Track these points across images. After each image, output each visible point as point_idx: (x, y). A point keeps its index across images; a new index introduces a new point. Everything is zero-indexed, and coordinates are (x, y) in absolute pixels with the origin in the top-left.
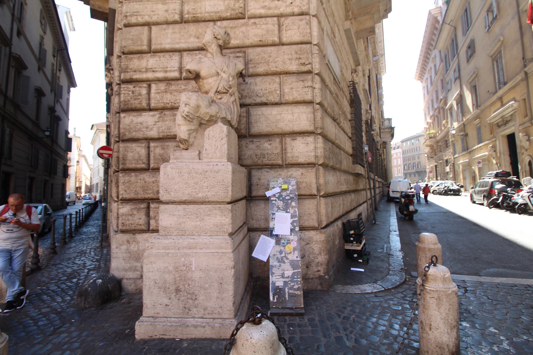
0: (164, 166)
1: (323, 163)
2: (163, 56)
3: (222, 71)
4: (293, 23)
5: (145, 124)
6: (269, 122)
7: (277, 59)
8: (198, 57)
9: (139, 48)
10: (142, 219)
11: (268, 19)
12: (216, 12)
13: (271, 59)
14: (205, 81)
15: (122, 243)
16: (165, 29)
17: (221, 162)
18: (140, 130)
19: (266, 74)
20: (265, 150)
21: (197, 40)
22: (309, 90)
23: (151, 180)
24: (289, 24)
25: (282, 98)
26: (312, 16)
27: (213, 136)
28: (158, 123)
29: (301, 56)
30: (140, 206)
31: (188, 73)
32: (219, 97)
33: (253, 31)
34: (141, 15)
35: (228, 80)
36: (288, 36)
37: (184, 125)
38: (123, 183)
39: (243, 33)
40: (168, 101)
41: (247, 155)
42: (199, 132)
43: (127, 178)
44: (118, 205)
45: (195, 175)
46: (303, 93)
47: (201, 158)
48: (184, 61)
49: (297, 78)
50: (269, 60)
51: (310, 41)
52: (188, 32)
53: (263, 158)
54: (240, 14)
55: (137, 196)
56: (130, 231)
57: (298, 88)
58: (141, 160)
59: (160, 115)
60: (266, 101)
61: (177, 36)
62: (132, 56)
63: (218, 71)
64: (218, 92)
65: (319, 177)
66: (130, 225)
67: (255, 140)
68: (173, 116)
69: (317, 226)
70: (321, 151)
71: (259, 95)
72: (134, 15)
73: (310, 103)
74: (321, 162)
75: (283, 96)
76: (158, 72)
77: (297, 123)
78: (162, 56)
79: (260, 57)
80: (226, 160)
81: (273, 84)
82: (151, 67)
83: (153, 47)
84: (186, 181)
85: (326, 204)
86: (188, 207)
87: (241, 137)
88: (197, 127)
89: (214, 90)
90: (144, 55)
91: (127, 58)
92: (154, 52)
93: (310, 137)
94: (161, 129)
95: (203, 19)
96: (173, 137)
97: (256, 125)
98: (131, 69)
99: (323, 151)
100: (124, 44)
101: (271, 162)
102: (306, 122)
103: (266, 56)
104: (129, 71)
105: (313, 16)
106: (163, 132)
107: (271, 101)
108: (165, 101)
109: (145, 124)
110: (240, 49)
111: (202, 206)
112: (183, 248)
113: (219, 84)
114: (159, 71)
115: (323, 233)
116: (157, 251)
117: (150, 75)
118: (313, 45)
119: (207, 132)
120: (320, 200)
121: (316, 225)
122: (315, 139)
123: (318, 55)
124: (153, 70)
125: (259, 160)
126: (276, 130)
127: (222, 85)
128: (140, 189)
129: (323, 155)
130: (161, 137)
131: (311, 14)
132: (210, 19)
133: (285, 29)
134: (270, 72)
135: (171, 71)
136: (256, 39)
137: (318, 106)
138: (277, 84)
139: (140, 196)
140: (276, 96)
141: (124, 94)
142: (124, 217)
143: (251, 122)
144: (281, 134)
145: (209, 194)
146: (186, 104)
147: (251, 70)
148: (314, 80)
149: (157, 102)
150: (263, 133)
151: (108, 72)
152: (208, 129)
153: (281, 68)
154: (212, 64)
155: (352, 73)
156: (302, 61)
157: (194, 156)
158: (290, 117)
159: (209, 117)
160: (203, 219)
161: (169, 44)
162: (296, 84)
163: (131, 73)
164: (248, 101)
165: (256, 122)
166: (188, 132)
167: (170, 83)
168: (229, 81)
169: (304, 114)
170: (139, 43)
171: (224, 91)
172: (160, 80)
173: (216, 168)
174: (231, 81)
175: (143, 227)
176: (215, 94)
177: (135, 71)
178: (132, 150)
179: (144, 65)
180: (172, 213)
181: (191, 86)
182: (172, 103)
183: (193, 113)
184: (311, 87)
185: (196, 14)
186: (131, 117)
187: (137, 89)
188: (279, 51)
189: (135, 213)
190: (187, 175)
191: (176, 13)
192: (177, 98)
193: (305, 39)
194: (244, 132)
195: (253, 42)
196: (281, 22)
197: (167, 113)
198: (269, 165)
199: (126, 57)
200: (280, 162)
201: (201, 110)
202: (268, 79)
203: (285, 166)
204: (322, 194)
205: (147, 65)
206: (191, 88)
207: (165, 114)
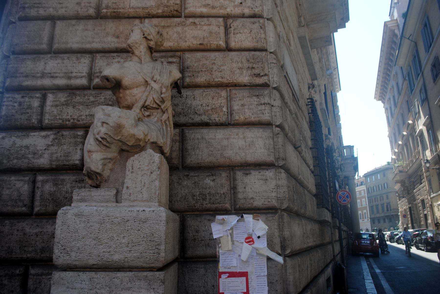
0: (63, 212)
1: (288, 207)
2: (68, 58)
4: (243, 25)
5: (31, 149)
6: (212, 149)
7: (222, 68)
8: (116, 60)
9: (36, 47)
11: (211, 19)
12: (143, 8)
13: (215, 67)
14: (128, 92)
16: (74, 25)
18: (24, 156)
19: (208, 86)
20: (206, 188)
21: (116, 40)
22: (266, 108)
23: (35, 231)
24: (238, 26)
26: (266, 19)
27: (140, 168)
28: (52, 148)
29: (254, 66)
31: (105, 80)
32: (147, 113)
33: (191, 32)
34: (44, 7)
35: (159, 92)
36: (237, 40)
37: (97, 151)
39: (178, 33)
40: (69, 117)
41: (180, 196)
48: (96, 65)
49: (250, 93)
50: (212, 68)
51: (265, 48)
53: (203, 199)
54: (175, 12)
58: (20, 200)
59: (55, 136)
60: (208, 121)
62: (25, 57)
63: (147, 80)
64: (146, 107)
65: (282, 228)
67: (192, 174)
68: (75, 137)
72: (34, 7)
73: (267, 125)
74: (285, 206)
75: (231, 115)
76: (58, 78)
78: (66, 58)
79: (201, 64)
80: (157, 204)
81: (218, 99)
82: (49, 72)
83: (55, 46)
86: (95, 276)
87: (173, 169)
89: (140, 104)
92: (55, 53)
93: (270, 171)
94: (55, 156)
95: (126, 15)
97: (193, 153)
98: (22, 73)
99: (286, 190)
101: (214, 206)
102: (263, 150)
103: (207, 63)
104: (18, 75)
106: (58, 160)
107: (214, 121)
108: (65, 117)
109: (31, 149)
110: (173, 53)
111: (120, 274)
114: (60, 77)
117: (47, 82)
119: (129, 163)
124: (52, 75)
126: (222, 161)
127: (151, 98)
129: (287, 196)
130: (54, 167)
131: (265, 17)
132: (135, 15)
133: (233, 32)
134: (214, 83)
135: (76, 77)
136: (195, 42)
140: (221, 114)
141: (7, 105)
144: (229, 166)
145: (129, 255)
146: (103, 123)
147: (187, 80)
148: (272, 95)
149: (52, 118)
152: (132, 158)
153: (228, 78)
155: (309, 88)
156: (257, 71)
158: (241, 143)
159: (134, 141)
161: (77, 43)
162: (248, 99)
163: (21, 79)
164: (182, 120)
166: (102, 161)
167: (73, 93)
168: (161, 93)
169: (259, 139)
170: (36, 41)
171: (155, 106)
174: (164, 93)
176: (141, 110)
177: (27, 76)
179: (40, 69)
181: (103, 98)
182: (74, 119)
185: (117, 9)
187: (27, 99)
188: (225, 58)
190: (97, 225)
191: (90, 7)
192: (82, 113)
193: (259, 45)
194: (175, 162)
195: (191, 45)
197: (66, 133)
198: (212, 211)
199: (16, 58)
201: (124, 131)
202: (211, 92)
205: (45, 69)
207: (62, 135)
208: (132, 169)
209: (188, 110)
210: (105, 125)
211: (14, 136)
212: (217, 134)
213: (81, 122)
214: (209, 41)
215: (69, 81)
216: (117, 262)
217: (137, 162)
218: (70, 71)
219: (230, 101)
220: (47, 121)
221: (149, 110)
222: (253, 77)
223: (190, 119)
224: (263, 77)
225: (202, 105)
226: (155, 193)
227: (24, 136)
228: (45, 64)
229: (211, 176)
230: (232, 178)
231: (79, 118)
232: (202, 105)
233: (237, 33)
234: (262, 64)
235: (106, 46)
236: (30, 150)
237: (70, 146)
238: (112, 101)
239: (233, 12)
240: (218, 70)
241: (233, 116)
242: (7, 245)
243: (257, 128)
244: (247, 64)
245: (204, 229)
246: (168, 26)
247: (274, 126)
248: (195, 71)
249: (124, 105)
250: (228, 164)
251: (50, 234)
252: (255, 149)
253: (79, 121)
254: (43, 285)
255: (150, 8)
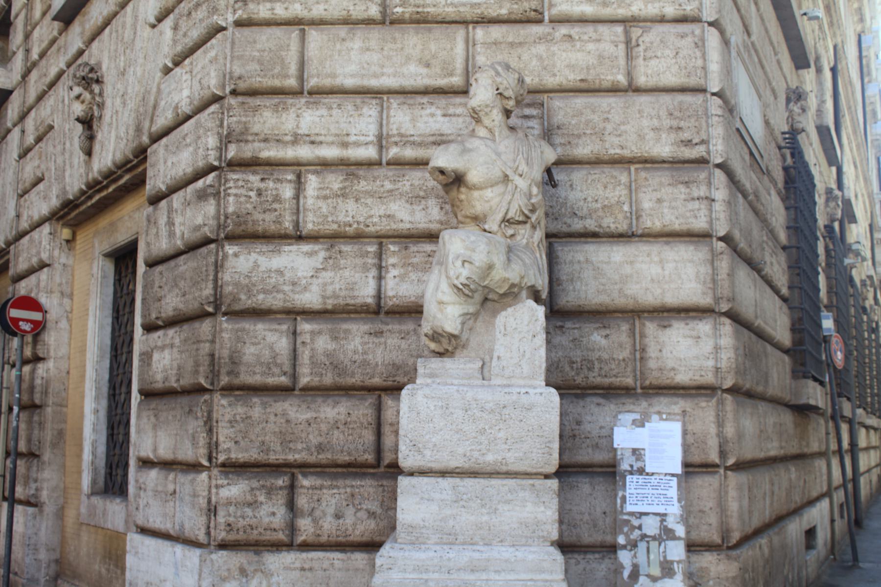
0: (409, 392)
1: (734, 385)
3: (515, 172)
4: (662, 41)
5: (288, 275)
6: (604, 281)
7: (622, 128)
8: (428, 111)
9: (277, 83)
10: (279, 516)
13: (609, 127)
14: (476, 194)
15: (226, 574)
16: (343, 40)
17: (535, 388)
18: (276, 289)
19: (597, 162)
20: (593, 350)
21: (424, 71)
24: (652, 43)
25: (634, 221)
26: (706, 25)
27: (516, 329)
28: (324, 274)
29: (682, 124)
30: (273, 481)
32: (510, 232)
33: (564, 54)
36: (650, 72)
37: (454, 303)
38: (230, 422)
39: (540, 58)
40: (349, 219)
42: (480, 318)
43: (240, 410)
44: (210, 477)
45: (478, 414)
46: (688, 214)
47: (486, 374)
48: (392, 120)
49: (672, 176)
50: (604, 129)
51: (704, 87)
52: (402, 49)
53: (589, 369)
54: (533, 13)
55: (266, 457)
56: (245, 545)
57: (675, 199)
59: (328, 254)
60: (597, 229)
61: (375, 57)
64: (508, 221)
65: (723, 421)
66: (249, 530)
67: (569, 324)
68: (362, 256)
69: (719, 541)
70: (729, 355)
71: (579, 214)
74: (728, 384)
75: (637, 218)
77: (672, 286)
78: (335, 106)
79: (583, 120)
80: (544, 383)
81: (614, 188)
84: (459, 427)
85: (740, 488)
86: (461, 484)
88: (478, 307)
89: (499, 216)
90: (290, 101)
91: (246, 106)
92: (310, 93)
94: (330, 289)
96: (359, 309)
97: (571, 288)
98: (257, 134)
100: (238, 71)
101: (607, 381)
102: (693, 285)
103: (595, 118)
104: (250, 138)
105: (711, 24)
106: (335, 296)
107: (608, 230)
108: (341, 218)
109: (288, 275)
111: (495, 482)
112: (459, 570)
113: (509, 203)
114: (327, 143)
115: (735, 559)
116: (401, 575)
117: (304, 152)
118: (709, 96)
120: (725, 477)
121: (717, 539)
122: (715, 328)
123: (721, 119)
124: (312, 139)
125: (578, 374)
126: (620, 302)
127: (517, 206)
128: (273, 438)
130: (330, 307)
131: (704, 19)
132: (458, 19)
133: (642, 54)
134: (606, 158)
136: (572, 77)
137: (721, 244)
138: (622, 187)
139: (272, 458)
141: (236, 195)
142: (232, 509)
143: (558, 279)
144: (632, 311)
145: (509, 455)
146: (464, 261)
149: (320, 220)
150: (587, 308)
151: (86, 89)
152: (503, 313)
153: (632, 149)
154: (494, 157)
155: (788, 100)
156: (686, 136)
157: (471, 371)
158: (655, 270)
160: (496, 509)
161: (352, 76)
162: (670, 190)
163: (256, 144)
165: (572, 280)
167: (353, 174)
169: (689, 265)
171: (521, 219)
172: (325, 165)
173: (524, 399)
174: (536, 196)
175: (281, 536)
176: (500, 226)
177: (266, 140)
178: (254, 340)
179: (290, 127)
180: (426, 496)
182: (358, 223)
183: (477, 280)
184: (707, 198)
186: (254, 256)
187: (271, 184)
188: (627, 108)
189: (262, 498)
192: (372, 212)
193: (693, 82)
195: (565, 82)
196: (634, 37)
197: (346, 248)
198: (603, 388)
200: (629, 381)
203: (639, 391)
204: (731, 462)
205: (297, 126)
206: (407, 188)
207: (340, 252)
208: (505, 329)
209: (561, 208)
210: (466, 264)
211: (255, 252)
212: (612, 254)
213: (372, 229)
214: (598, 75)
215: (345, 152)
216: (490, 464)
217: (512, 319)
218: (345, 132)
219: (636, 190)
220: (310, 226)
221: (513, 226)
222: (679, 146)
223: (564, 226)
224: (697, 147)
225: (585, 199)
226: (540, 367)
227: (273, 251)
228: (298, 116)
229: (603, 330)
230: (637, 331)
231: (368, 220)
232: (585, 199)
233: (650, 58)
234: (697, 120)
235: (408, 83)
236: (286, 278)
237: (356, 272)
238: (425, 191)
239: (643, 13)
240: (615, 132)
241: (641, 220)
242: (259, 439)
243: (685, 242)
244: (668, 121)
245: (589, 418)
246: (520, 43)
247: (714, 239)
248: (573, 134)
249: (468, 214)
250: (631, 308)
251: (332, 422)
252: (679, 282)
253: (368, 226)
254: (324, 504)
255: (485, 6)
